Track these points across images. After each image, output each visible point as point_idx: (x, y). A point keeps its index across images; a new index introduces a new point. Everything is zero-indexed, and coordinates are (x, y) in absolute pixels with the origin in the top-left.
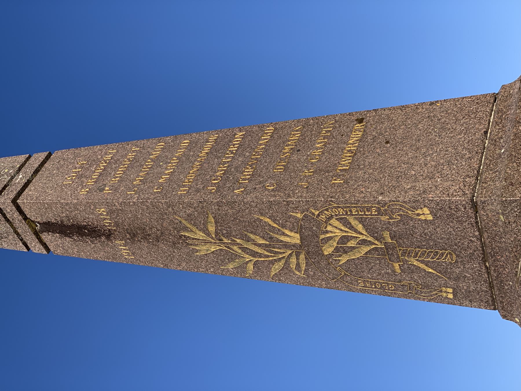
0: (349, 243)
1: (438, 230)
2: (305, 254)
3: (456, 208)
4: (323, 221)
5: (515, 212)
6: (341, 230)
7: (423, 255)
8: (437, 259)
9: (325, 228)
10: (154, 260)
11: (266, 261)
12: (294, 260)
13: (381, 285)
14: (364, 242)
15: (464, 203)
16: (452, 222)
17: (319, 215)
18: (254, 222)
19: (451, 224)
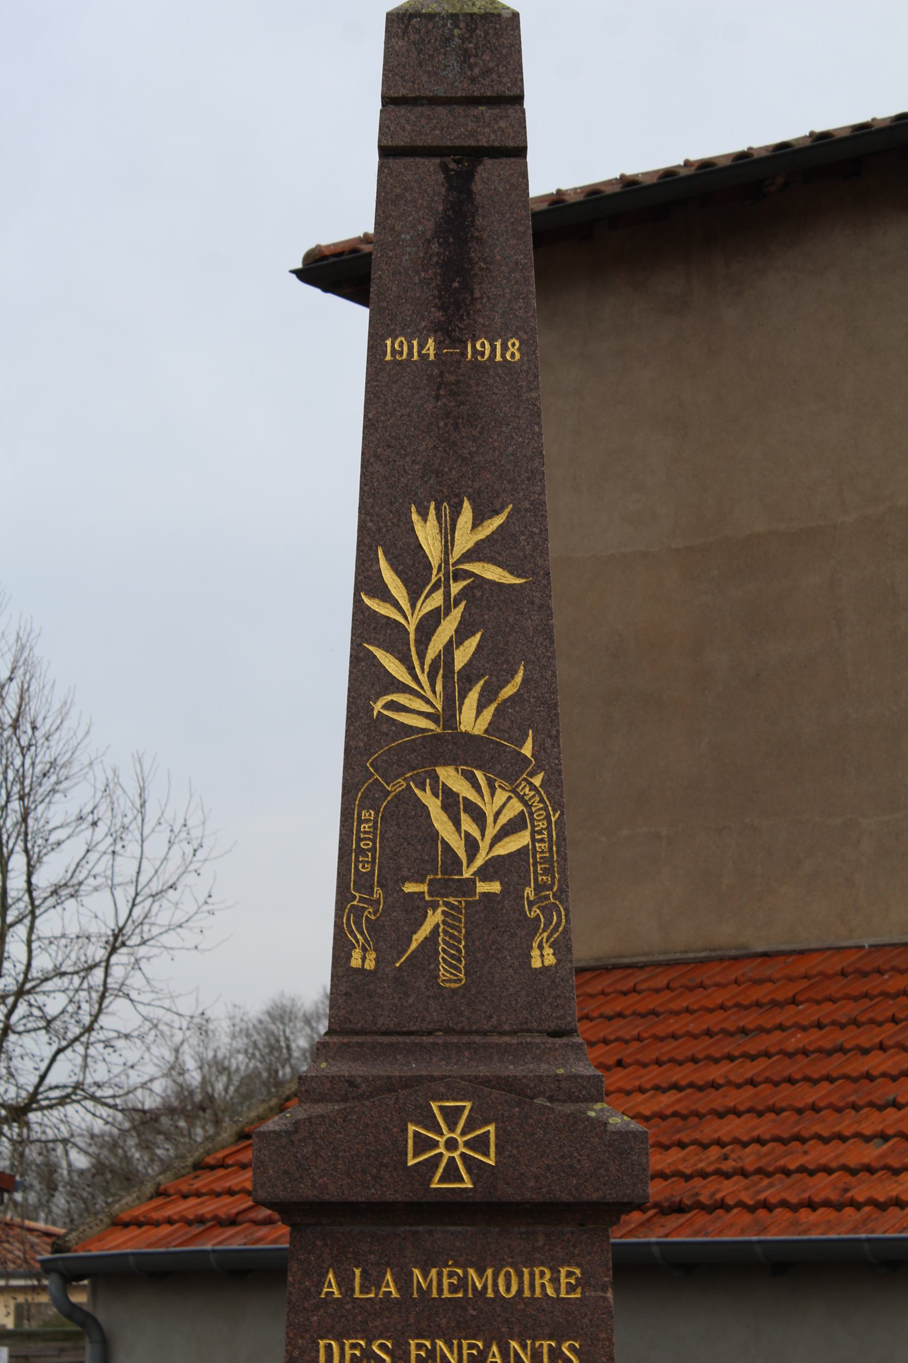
0: (469, 819)
1: (510, 970)
2: (433, 731)
3: (557, 1006)
4: (517, 786)
5: (580, 1091)
6: (497, 814)
7: (452, 937)
8: (443, 958)
9: (500, 786)
10: (386, 404)
11: (409, 649)
12: (418, 705)
13: (368, 850)
14: (472, 847)
15: (569, 1019)
16: (527, 995)
17: (531, 784)
18: (507, 661)
19: (524, 993)
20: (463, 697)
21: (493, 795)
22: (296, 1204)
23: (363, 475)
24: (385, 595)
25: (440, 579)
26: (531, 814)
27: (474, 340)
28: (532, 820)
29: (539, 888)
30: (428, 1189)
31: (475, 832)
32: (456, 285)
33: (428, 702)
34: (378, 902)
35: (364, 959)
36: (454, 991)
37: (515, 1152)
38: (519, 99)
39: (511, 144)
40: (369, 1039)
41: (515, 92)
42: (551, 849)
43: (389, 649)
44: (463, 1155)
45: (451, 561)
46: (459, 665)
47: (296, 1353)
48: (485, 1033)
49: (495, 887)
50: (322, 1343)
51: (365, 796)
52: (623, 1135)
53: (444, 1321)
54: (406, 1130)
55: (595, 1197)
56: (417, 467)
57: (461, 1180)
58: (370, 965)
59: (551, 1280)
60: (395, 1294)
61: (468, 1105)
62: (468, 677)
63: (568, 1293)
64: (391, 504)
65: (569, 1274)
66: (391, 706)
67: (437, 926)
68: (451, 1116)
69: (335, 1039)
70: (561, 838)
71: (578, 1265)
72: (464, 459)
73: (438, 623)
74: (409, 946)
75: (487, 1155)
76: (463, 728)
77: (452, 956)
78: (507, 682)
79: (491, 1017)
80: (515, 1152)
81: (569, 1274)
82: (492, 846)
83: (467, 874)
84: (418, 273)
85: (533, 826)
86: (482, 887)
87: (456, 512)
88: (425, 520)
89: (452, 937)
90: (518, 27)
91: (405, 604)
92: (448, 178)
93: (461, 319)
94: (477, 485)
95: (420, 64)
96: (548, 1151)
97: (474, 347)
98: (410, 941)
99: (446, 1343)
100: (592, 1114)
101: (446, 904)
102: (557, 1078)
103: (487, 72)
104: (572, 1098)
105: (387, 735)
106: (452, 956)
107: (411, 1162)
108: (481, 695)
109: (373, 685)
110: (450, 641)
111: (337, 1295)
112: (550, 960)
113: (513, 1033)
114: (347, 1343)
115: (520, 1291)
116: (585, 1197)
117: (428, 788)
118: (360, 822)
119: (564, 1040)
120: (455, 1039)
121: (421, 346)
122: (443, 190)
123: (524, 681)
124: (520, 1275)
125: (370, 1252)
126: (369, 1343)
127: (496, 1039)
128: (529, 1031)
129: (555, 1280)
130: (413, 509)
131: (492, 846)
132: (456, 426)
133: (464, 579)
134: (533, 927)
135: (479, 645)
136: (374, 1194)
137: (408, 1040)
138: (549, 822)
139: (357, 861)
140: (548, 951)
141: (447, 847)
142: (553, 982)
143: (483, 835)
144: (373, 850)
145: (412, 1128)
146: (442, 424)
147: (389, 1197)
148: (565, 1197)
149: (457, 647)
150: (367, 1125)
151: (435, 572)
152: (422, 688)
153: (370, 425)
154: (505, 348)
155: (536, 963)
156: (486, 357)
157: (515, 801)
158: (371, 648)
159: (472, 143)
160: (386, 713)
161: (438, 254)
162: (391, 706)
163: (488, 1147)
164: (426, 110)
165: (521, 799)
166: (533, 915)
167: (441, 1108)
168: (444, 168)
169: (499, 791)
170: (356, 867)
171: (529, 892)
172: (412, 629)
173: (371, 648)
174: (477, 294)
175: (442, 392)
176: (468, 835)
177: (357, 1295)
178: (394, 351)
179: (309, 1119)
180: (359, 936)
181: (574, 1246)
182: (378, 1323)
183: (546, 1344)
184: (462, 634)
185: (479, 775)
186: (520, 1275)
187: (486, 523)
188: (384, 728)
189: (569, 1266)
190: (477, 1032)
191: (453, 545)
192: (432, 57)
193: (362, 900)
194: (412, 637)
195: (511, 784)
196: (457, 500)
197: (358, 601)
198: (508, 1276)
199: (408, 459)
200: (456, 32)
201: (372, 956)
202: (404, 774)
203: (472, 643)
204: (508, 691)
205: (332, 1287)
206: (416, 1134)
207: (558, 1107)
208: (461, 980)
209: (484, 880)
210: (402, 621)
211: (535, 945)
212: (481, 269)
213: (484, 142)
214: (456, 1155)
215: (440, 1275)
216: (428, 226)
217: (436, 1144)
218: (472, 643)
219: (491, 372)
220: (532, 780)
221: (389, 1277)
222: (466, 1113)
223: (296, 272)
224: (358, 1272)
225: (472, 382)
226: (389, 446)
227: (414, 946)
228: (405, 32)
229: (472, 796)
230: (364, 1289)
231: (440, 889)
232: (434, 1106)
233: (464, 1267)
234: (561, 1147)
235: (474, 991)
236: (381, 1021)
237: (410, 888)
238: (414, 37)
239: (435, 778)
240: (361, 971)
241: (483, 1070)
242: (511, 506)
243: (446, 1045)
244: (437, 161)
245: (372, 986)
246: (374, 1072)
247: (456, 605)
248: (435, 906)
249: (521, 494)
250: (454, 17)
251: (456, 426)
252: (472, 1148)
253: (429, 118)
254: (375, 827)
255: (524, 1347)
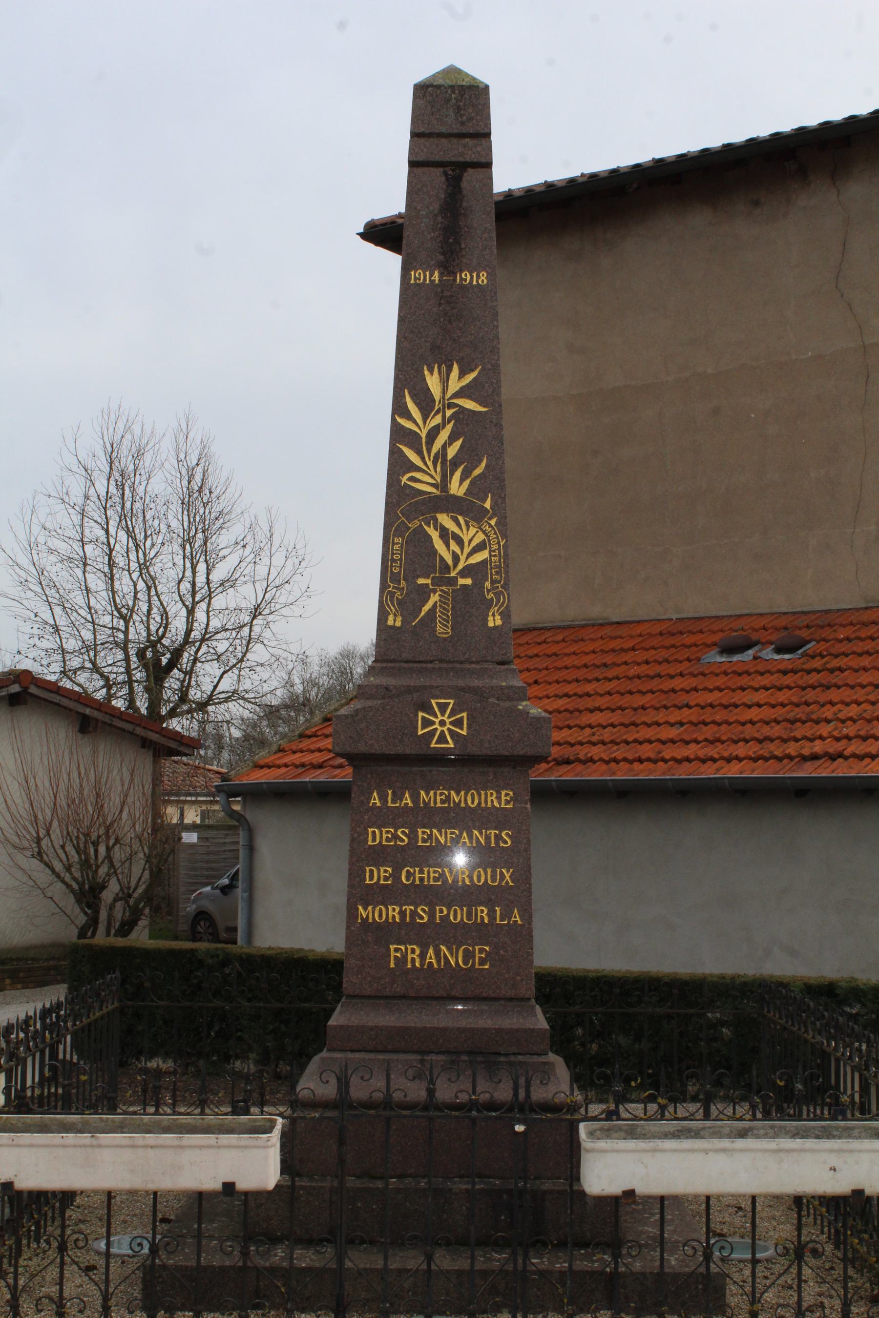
1: (476, 628)
6: (470, 541)
7: (444, 609)
14: (456, 558)
17: (489, 524)
18: (477, 455)
19: (483, 640)
20: (452, 475)
21: (468, 530)
22: (356, 754)
23: (397, 349)
24: (409, 417)
25: (440, 408)
26: (489, 541)
27: (461, 271)
28: (490, 544)
29: (493, 582)
30: (429, 747)
31: (457, 550)
32: (451, 240)
33: (432, 477)
34: (403, 588)
35: (395, 620)
36: (445, 639)
37: (478, 728)
38: (488, 135)
39: (483, 160)
40: (397, 665)
41: (486, 131)
42: (500, 560)
43: (411, 446)
44: (449, 729)
45: (446, 398)
46: (449, 457)
47: (356, 835)
48: (462, 662)
49: (468, 581)
50: (370, 830)
51: (396, 530)
52: (538, 719)
53: (437, 819)
54: (417, 715)
55: (521, 753)
56: (428, 344)
57: (448, 743)
58: (398, 624)
59: (496, 798)
60: (410, 804)
61: (452, 701)
62: (455, 463)
63: (505, 805)
64: (413, 365)
65: (506, 795)
66: (412, 479)
67: (436, 603)
68: (443, 708)
69: (379, 665)
70: (506, 555)
71: (512, 790)
72: (454, 340)
73: (438, 433)
74: (420, 614)
75: (462, 729)
76: (452, 492)
77: (444, 620)
78: (477, 467)
79: (465, 653)
80: (478, 728)
81: (506, 795)
82: (467, 558)
83: (453, 574)
84: (430, 233)
85: (490, 548)
86: (462, 581)
87: (449, 370)
88: (432, 374)
89: (444, 609)
90: (488, 94)
91: (420, 421)
92: (447, 179)
93: (454, 260)
94: (461, 355)
95: (432, 114)
96: (496, 727)
97: (461, 276)
98: (421, 610)
99: (438, 831)
100: (521, 707)
101: (441, 590)
102: (502, 688)
103: (470, 119)
104: (509, 698)
105: (409, 495)
106: (444, 620)
107: (420, 733)
108: (462, 474)
109: (402, 467)
110: (445, 443)
111: (378, 804)
112: (499, 622)
113: (478, 662)
114: (384, 830)
115: (480, 803)
116: (516, 753)
117: (432, 526)
118: (394, 544)
119: (506, 667)
120: (445, 665)
121: (431, 276)
122: (445, 187)
123: (487, 466)
124: (480, 795)
125: (397, 781)
126: (396, 831)
127: (467, 666)
128: (486, 661)
129: (499, 798)
130: (425, 368)
131: (467, 558)
132: (450, 321)
133: (454, 408)
134: (489, 604)
135: (461, 445)
136: (399, 750)
137: (419, 665)
138: (500, 546)
139: (392, 566)
140: (498, 617)
141: (442, 559)
142: (500, 634)
143: (462, 552)
144: (401, 560)
145: (421, 714)
146: (442, 320)
147: (408, 751)
148: (505, 753)
149: (449, 447)
150: (396, 712)
151: (437, 404)
152: (429, 469)
153: (402, 320)
154: (478, 277)
155: (491, 624)
156: (468, 282)
157: (480, 533)
158: (401, 446)
159: (461, 159)
160: (409, 483)
161: (441, 223)
162: (412, 479)
163: (463, 724)
164: (436, 141)
165: (484, 532)
166: (489, 597)
167: (437, 703)
168: (446, 174)
169: (471, 528)
170: (391, 569)
171: (488, 584)
172: (424, 436)
173: (401, 446)
174: (463, 246)
175: (442, 302)
176: (454, 553)
177: (390, 804)
178: (415, 278)
179: (364, 708)
180: (392, 608)
181: (510, 780)
182: (401, 820)
183: (493, 832)
184: (452, 439)
185: (460, 518)
186: (480, 795)
187: (466, 376)
188: (408, 491)
189: (507, 790)
190: (457, 662)
191: (447, 389)
192: (439, 110)
193: (394, 587)
194: (424, 440)
195: (478, 524)
196: (450, 363)
197: (393, 420)
198: (473, 795)
199: (423, 340)
200: (453, 96)
201: (399, 619)
202: (418, 518)
203: (457, 444)
204: (477, 472)
205: (375, 800)
206: (423, 718)
207: (502, 704)
208: (448, 633)
209: (463, 577)
210: (418, 431)
211: (490, 614)
212: (466, 232)
213: (468, 159)
214: (445, 729)
215: (435, 794)
216: (436, 207)
217: (433, 723)
218: (457, 444)
219: (470, 290)
220: (490, 522)
221: (407, 795)
222: (451, 706)
223: (360, 234)
224: (390, 792)
225: (460, 296)
226: (412, 332)
227: (423, 614)
228: (424, 95)
229: (456, 530)
230: (393, 801)
231: (437, 582)
232: (433, 702)
233: (449, 790)
234: (503, 725)
235: (456, 639)
236: (404, 655)
237: (421, 581)
238: (429, 98)
239: (436, 520)
240: (393, 627)
241: (461, 683)
242: (480, 367)
243: (440, 669)
244: (441, 169)
245: (399, 636)
246: (400, 683)
247: (449, 422)
248: (435, 592)
249: (487, 360)
250: (452, 87)
251: (450, 321)
252: (454, 726)
253: (437, 145)
254: (402, 547)
255: (481, 834)
